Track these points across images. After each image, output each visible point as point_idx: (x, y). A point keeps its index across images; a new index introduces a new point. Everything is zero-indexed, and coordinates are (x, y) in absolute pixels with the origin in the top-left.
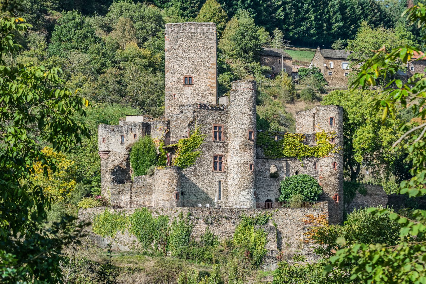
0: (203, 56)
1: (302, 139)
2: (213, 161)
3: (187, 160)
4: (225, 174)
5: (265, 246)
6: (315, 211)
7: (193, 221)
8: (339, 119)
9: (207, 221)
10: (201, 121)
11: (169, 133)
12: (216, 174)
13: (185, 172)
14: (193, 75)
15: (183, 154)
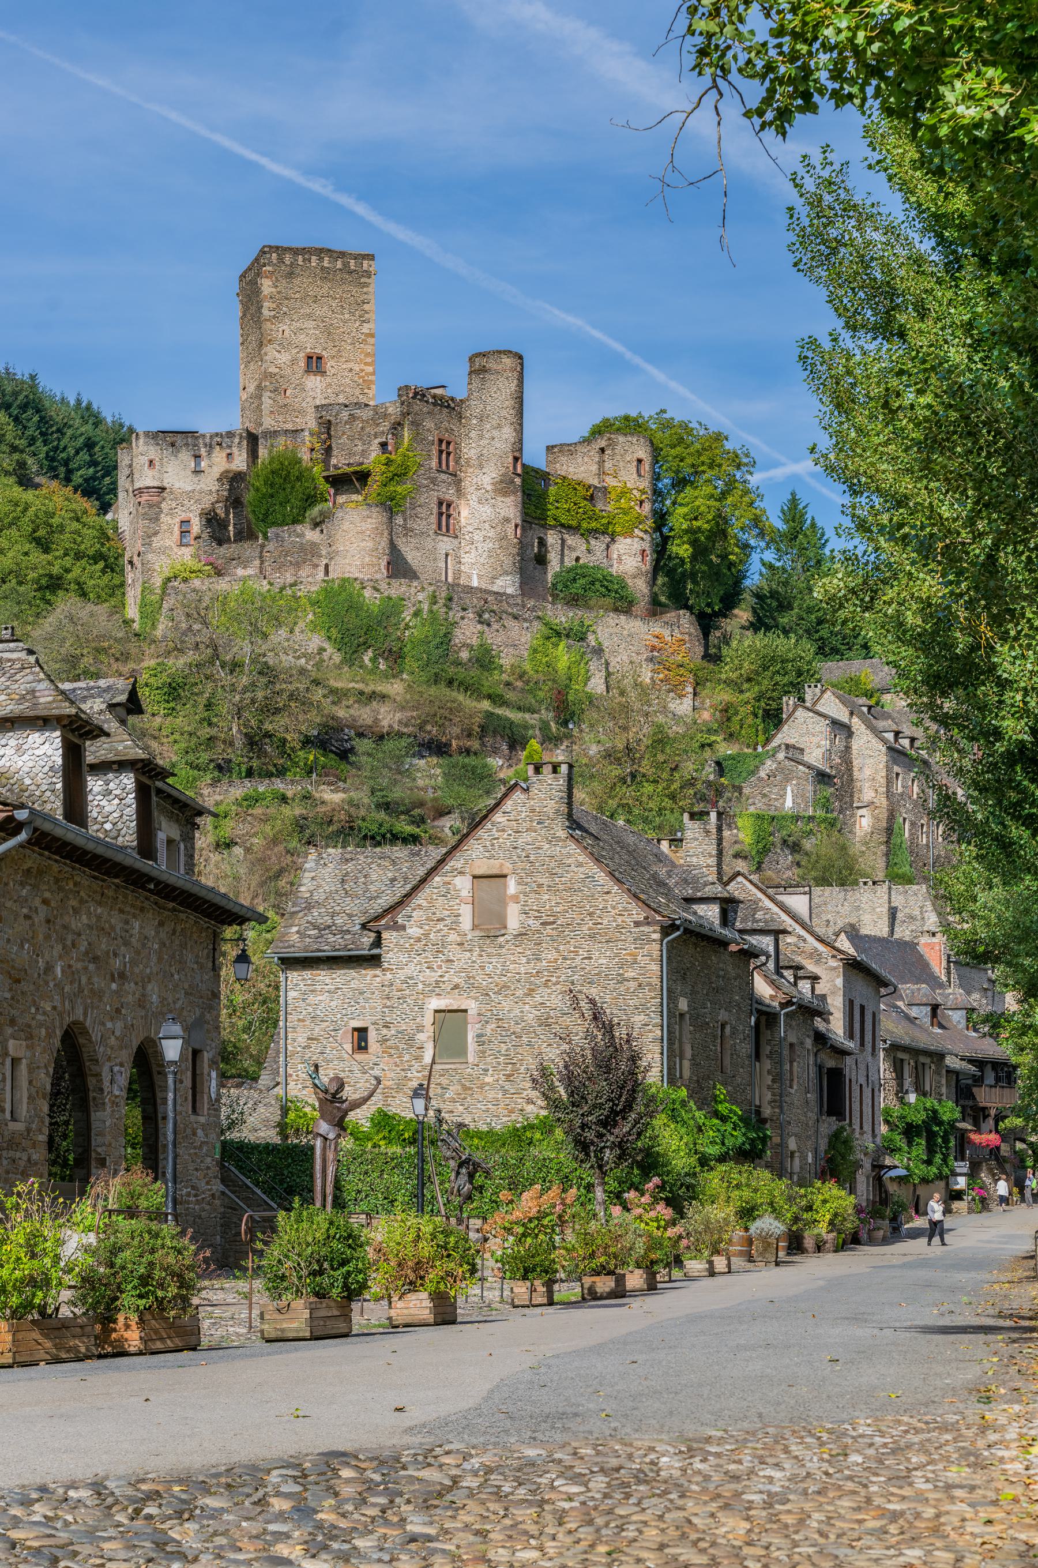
0: (347, 316)
2: (435, 511)
4: (456, 542)
5: (586, 684)
7: (455, 615)
10: (416, 424)
11: (329, 448)
14: (324, 353)
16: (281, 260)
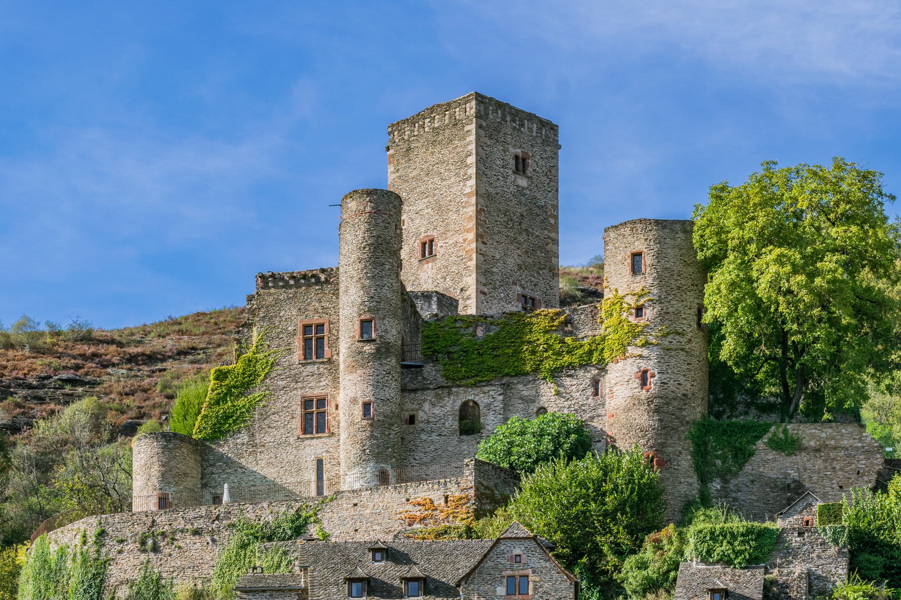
1: (556, 323)
2: (299, 411)
3: (228, 418)
4: (333, 440)
6: (436, 487)
7: (111, 548)
8: (659, 256)
9: (143, 543)
12: (307, 442)
13: (225, 449)
15: (217, 403)
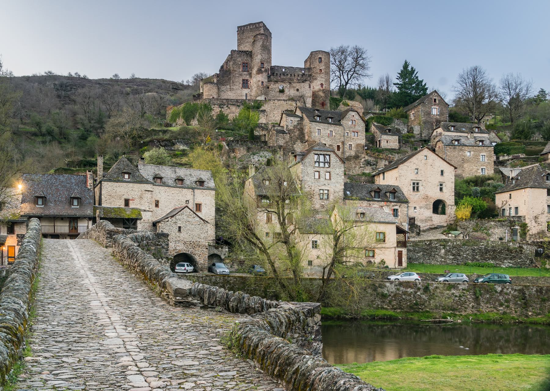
2: (241, 82)
4: (249, 90)
12: (244, 89)
16: (241, 29)
